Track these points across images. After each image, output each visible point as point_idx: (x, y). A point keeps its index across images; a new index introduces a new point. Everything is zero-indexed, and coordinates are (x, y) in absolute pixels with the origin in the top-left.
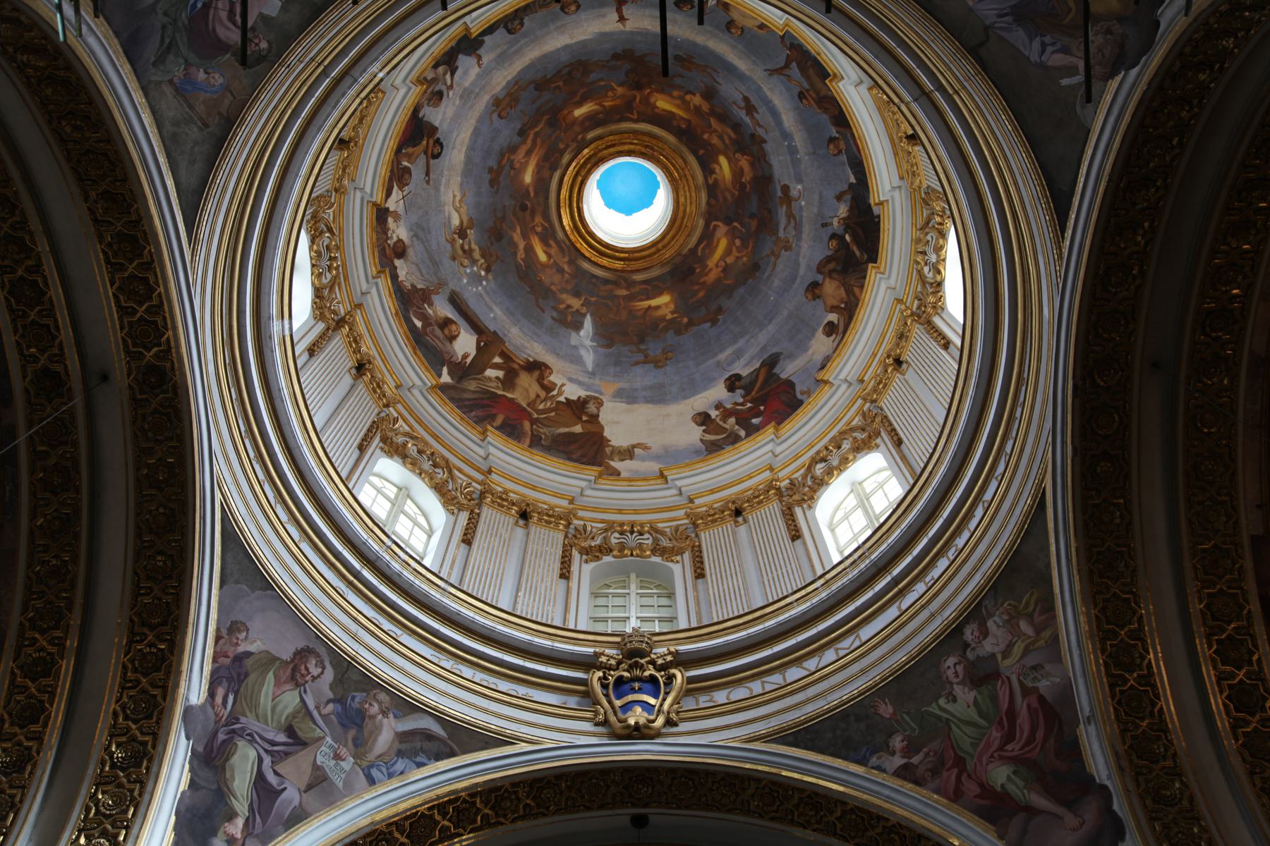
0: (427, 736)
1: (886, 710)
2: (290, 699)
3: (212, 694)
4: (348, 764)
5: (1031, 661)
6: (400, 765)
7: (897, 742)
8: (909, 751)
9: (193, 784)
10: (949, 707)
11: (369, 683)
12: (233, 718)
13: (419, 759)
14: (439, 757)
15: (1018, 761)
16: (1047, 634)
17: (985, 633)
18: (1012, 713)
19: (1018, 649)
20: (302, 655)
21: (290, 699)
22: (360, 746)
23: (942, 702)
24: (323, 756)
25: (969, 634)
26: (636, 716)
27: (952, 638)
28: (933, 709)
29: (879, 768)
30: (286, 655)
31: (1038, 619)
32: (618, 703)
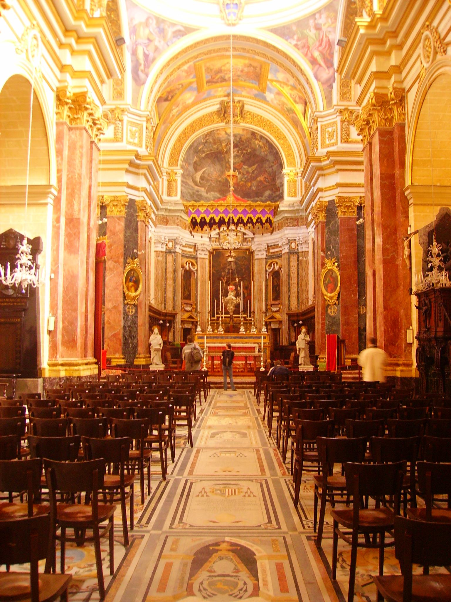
0: (180, 31)
1: (294, 28)
2: (147, 31)
3: (130, 38)
4: (162, 42)
5: (329, 29)
6: (174, 40)
7: (296, 37)
8: (298, 40)
9: (132, 61)
10: (309, 32)
11: (164, 21)
12: (136, 41)
13: (179, 37)
14: (183, 35)
15: (321, 53)
16: (334, 25)
17: (320, 17)
18: (322, 40)
19: (327, 25)
20: (148, 19)
21: (147, 31)
22: (164, 37)
23: (308, 30)
24: (156, 43)
25: (317, 16)
26: (232, 18)
27: (313, 16)
28: (305, 31)
29: (290, 43)
30: (143, 20)
31: (333, 20)
32: (227, 11)
